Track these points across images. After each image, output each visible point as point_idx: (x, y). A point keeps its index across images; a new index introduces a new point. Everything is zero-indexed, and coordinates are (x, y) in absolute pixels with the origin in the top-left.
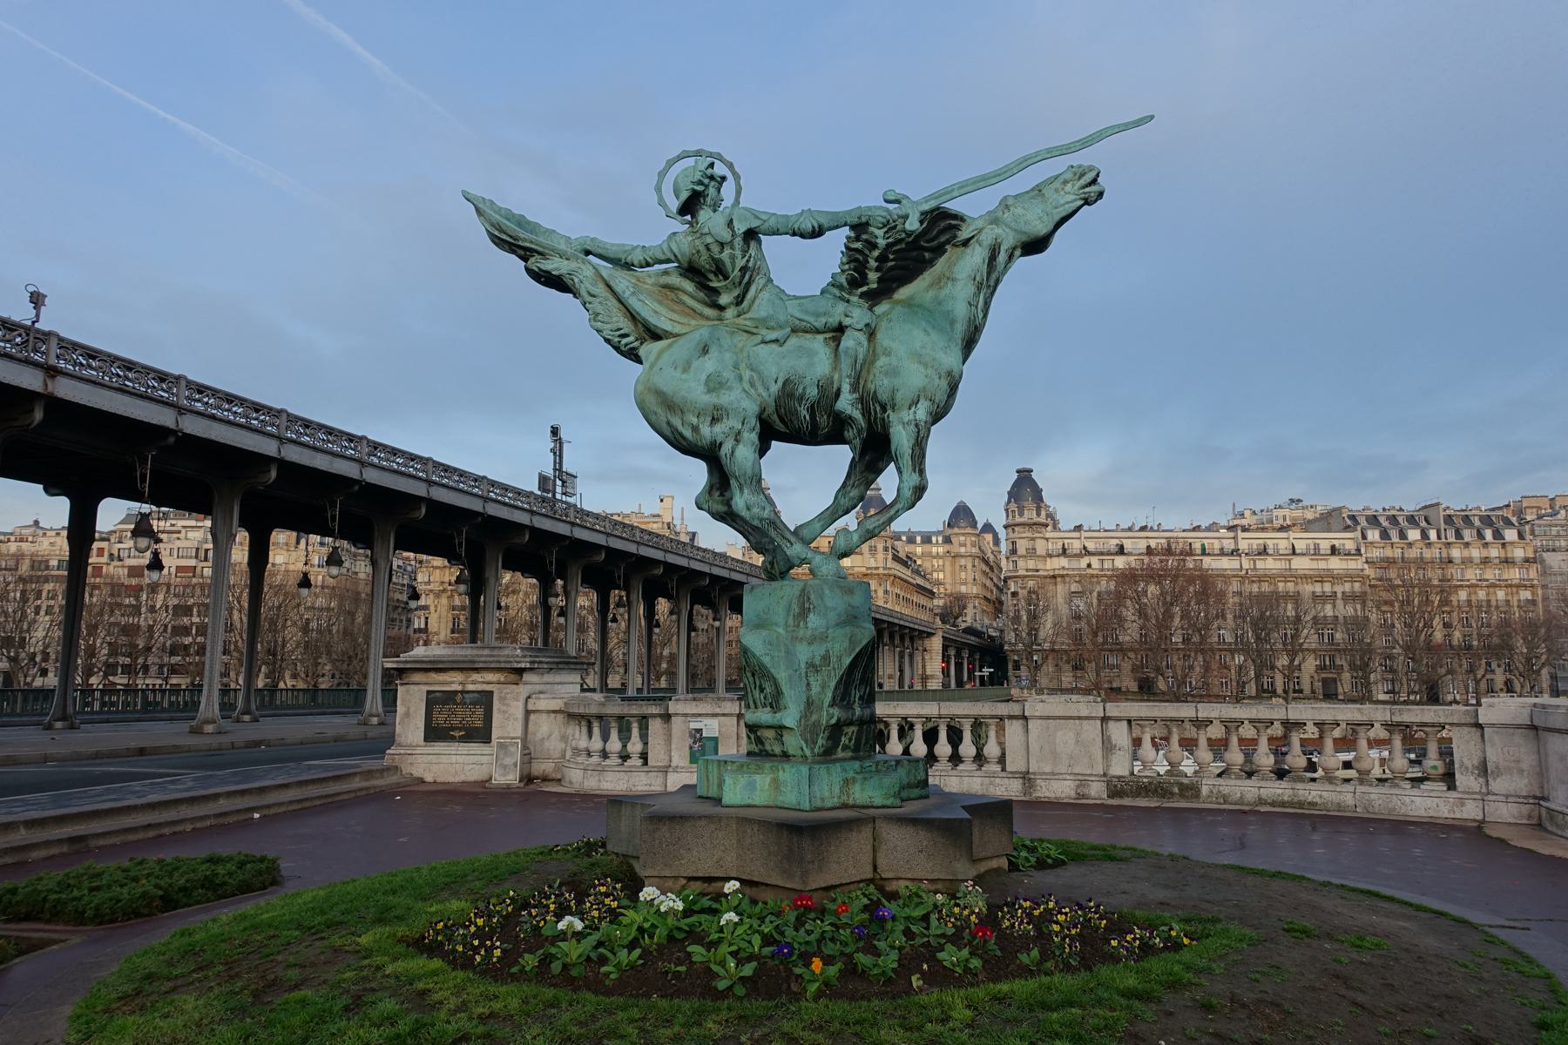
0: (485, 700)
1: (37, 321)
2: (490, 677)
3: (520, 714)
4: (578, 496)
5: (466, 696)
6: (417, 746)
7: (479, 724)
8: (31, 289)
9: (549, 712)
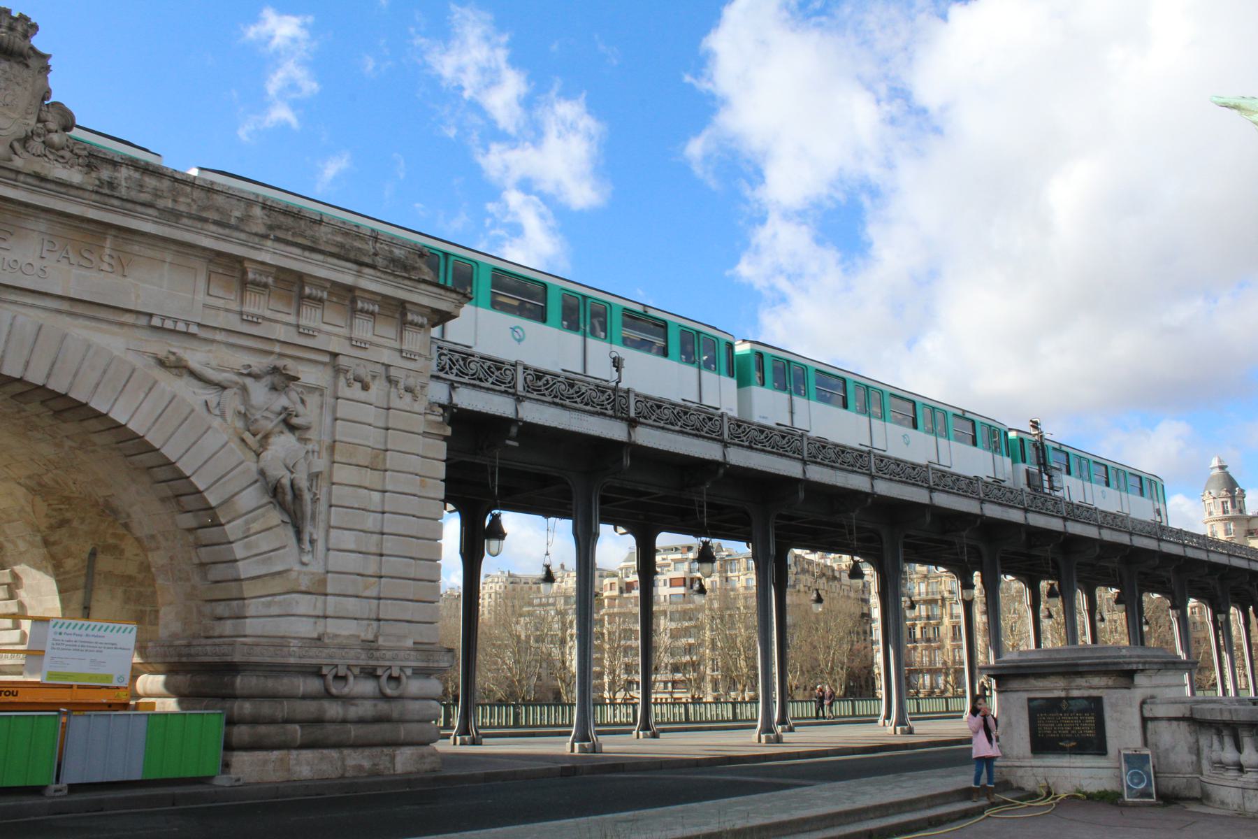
0: (1095, 706)
1: (620, 382)
2: (1096, 681)
3: (1137, 722)
4: (1066, 489)
5: (1072, 702)
6: (1024, 758)
7: (1090, 733)
8: (614, 355)
9: (1170, 719)
